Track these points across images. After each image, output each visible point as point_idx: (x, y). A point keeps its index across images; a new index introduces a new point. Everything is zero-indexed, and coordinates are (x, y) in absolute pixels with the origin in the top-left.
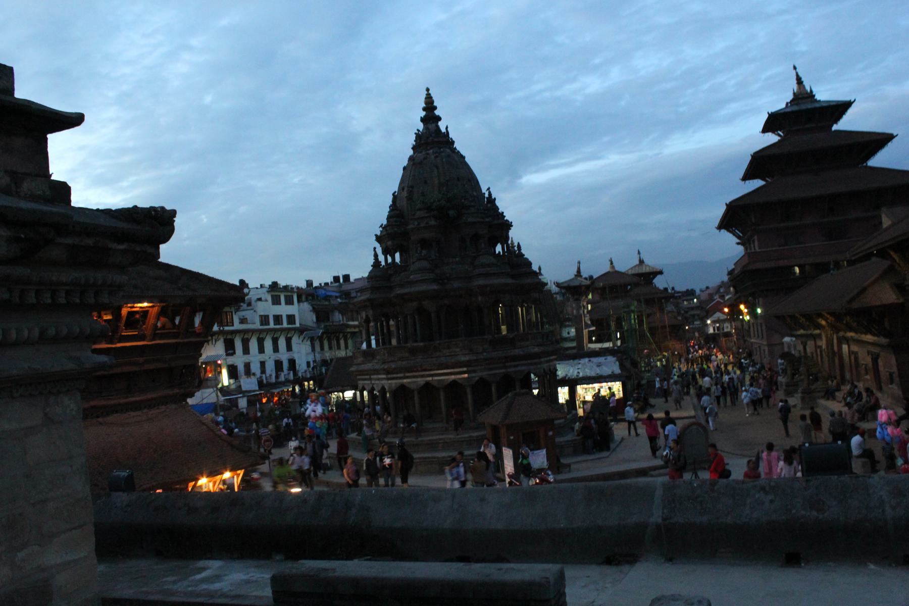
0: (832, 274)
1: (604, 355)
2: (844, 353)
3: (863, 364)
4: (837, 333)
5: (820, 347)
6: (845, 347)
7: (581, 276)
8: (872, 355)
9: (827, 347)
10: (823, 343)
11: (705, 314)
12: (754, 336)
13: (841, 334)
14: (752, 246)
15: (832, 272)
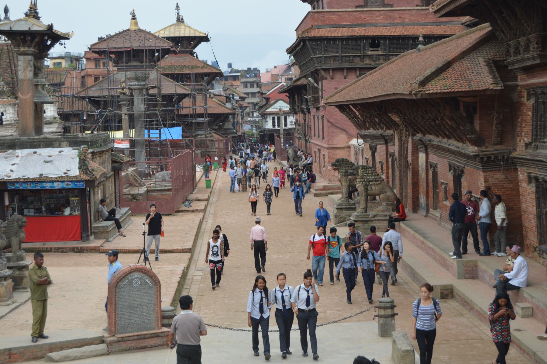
0: (419, 50)
1: (60, 146)
2: (420, 165)
3: (442, 183)
4: (414, 135)
5: (392, 155)
6: (422, 156)
7: (37, 18)
8: (455, 171)
9: (400, 155)
10: (395, 148)
11: (264, 102)
12: (315, 136)
13: (419, 136)
14: (320, 3)
15: (420, 46)
